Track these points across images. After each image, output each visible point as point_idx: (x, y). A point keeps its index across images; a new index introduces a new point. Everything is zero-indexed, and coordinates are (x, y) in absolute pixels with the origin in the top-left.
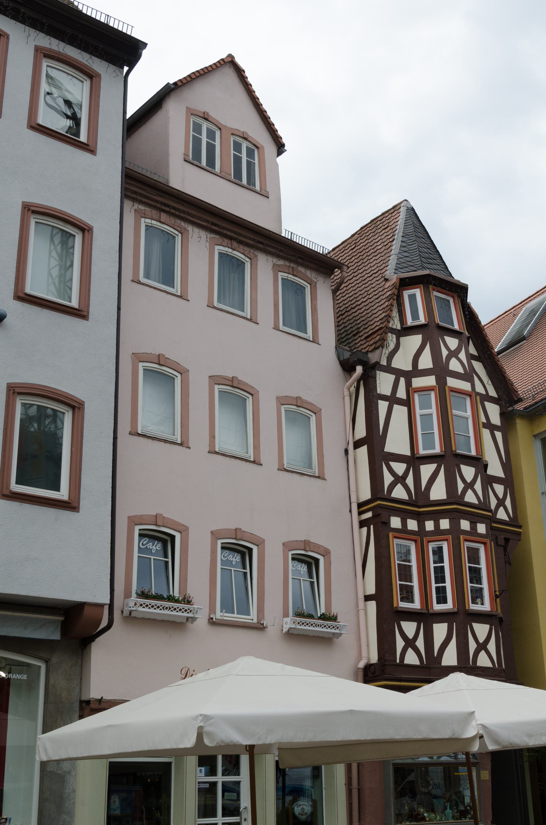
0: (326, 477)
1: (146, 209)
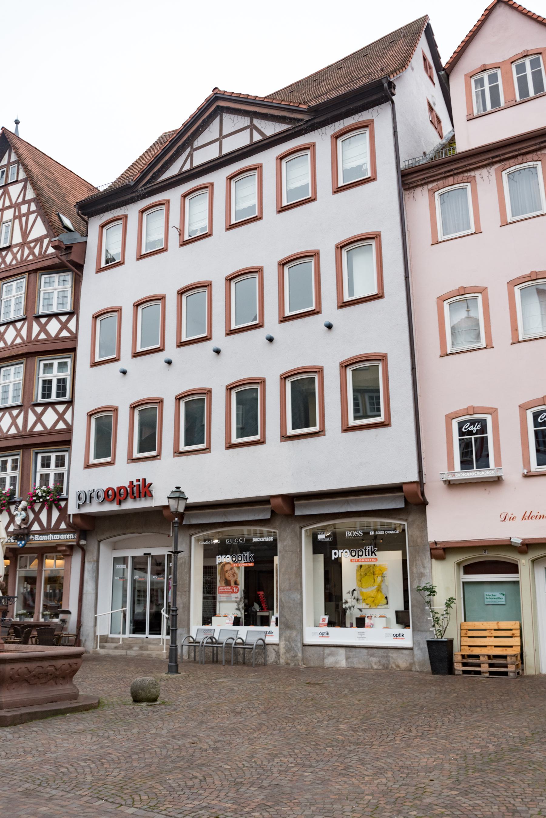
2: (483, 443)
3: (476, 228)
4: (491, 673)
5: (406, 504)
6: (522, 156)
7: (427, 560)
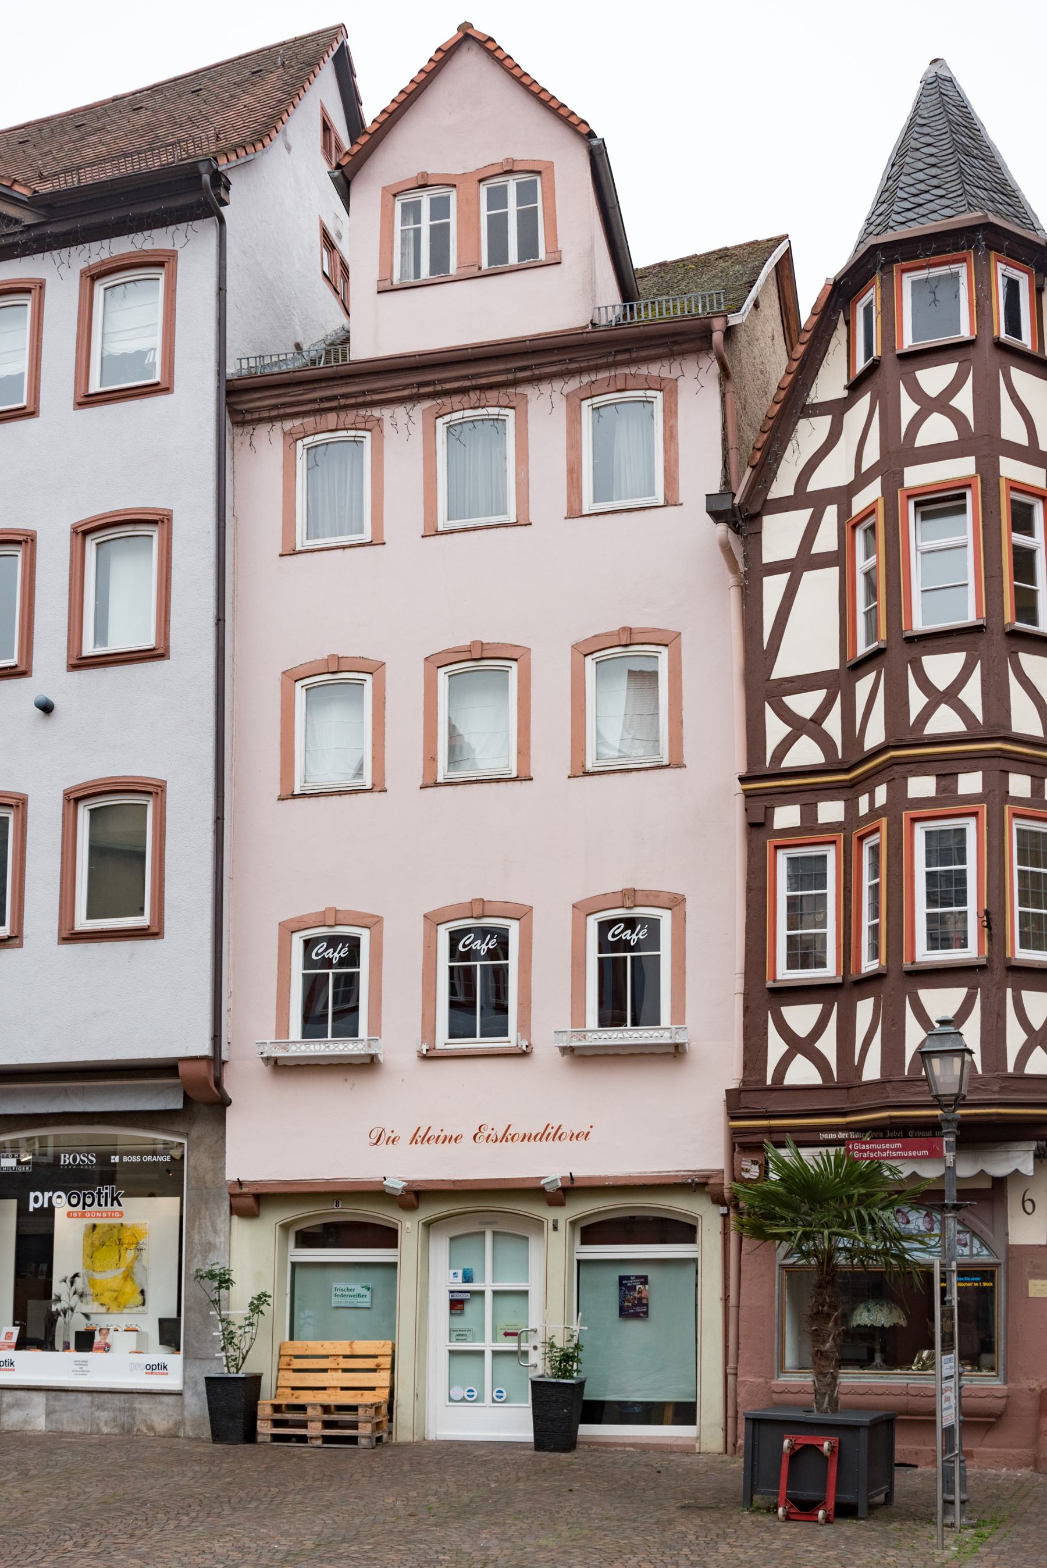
0: (685, 762)
1: (305, 420)
2: (348, 985)
3: (373, 533)
4: (327, 1439)
5: (185, 1103)
6: (478, 393)
7: (223, 1217)
